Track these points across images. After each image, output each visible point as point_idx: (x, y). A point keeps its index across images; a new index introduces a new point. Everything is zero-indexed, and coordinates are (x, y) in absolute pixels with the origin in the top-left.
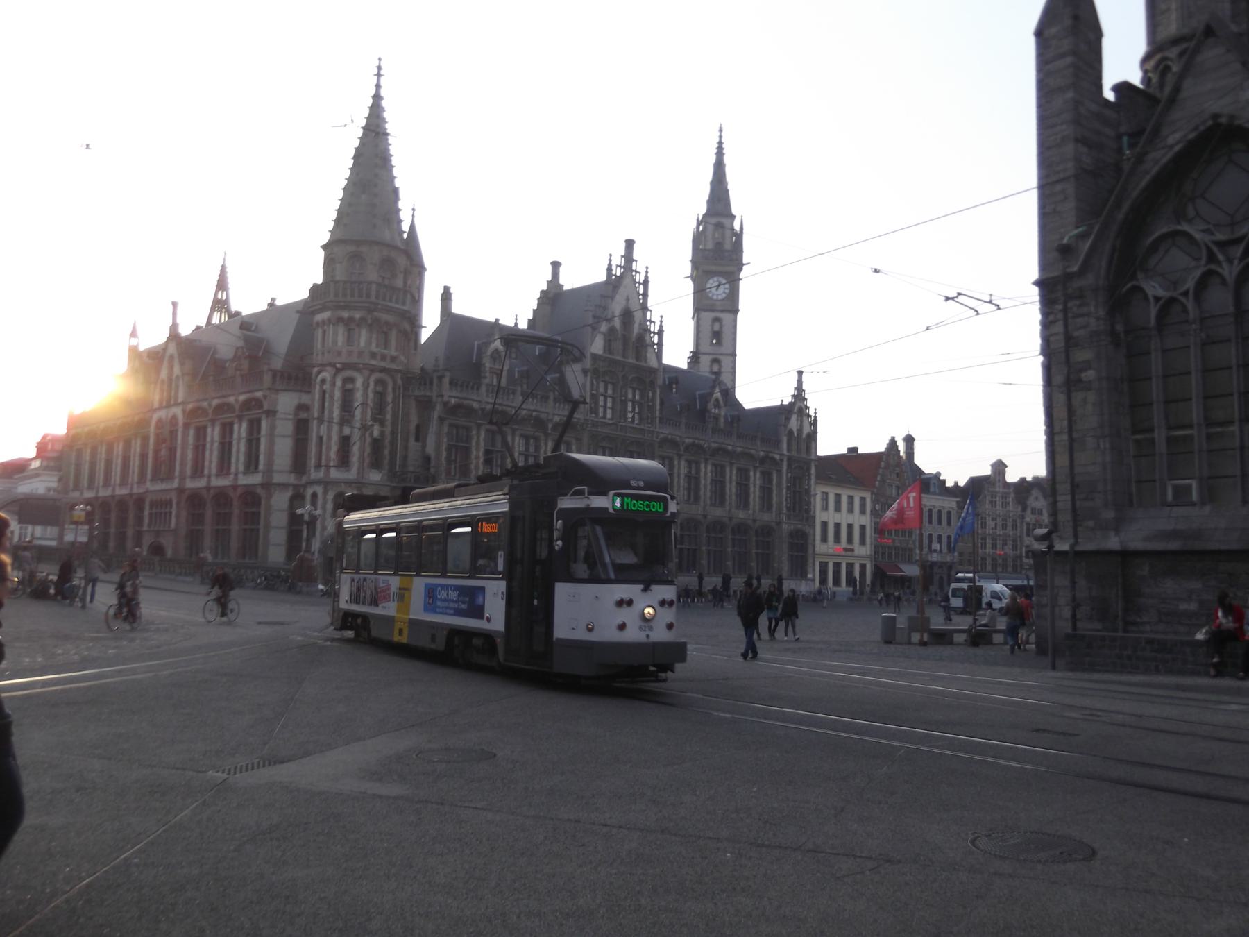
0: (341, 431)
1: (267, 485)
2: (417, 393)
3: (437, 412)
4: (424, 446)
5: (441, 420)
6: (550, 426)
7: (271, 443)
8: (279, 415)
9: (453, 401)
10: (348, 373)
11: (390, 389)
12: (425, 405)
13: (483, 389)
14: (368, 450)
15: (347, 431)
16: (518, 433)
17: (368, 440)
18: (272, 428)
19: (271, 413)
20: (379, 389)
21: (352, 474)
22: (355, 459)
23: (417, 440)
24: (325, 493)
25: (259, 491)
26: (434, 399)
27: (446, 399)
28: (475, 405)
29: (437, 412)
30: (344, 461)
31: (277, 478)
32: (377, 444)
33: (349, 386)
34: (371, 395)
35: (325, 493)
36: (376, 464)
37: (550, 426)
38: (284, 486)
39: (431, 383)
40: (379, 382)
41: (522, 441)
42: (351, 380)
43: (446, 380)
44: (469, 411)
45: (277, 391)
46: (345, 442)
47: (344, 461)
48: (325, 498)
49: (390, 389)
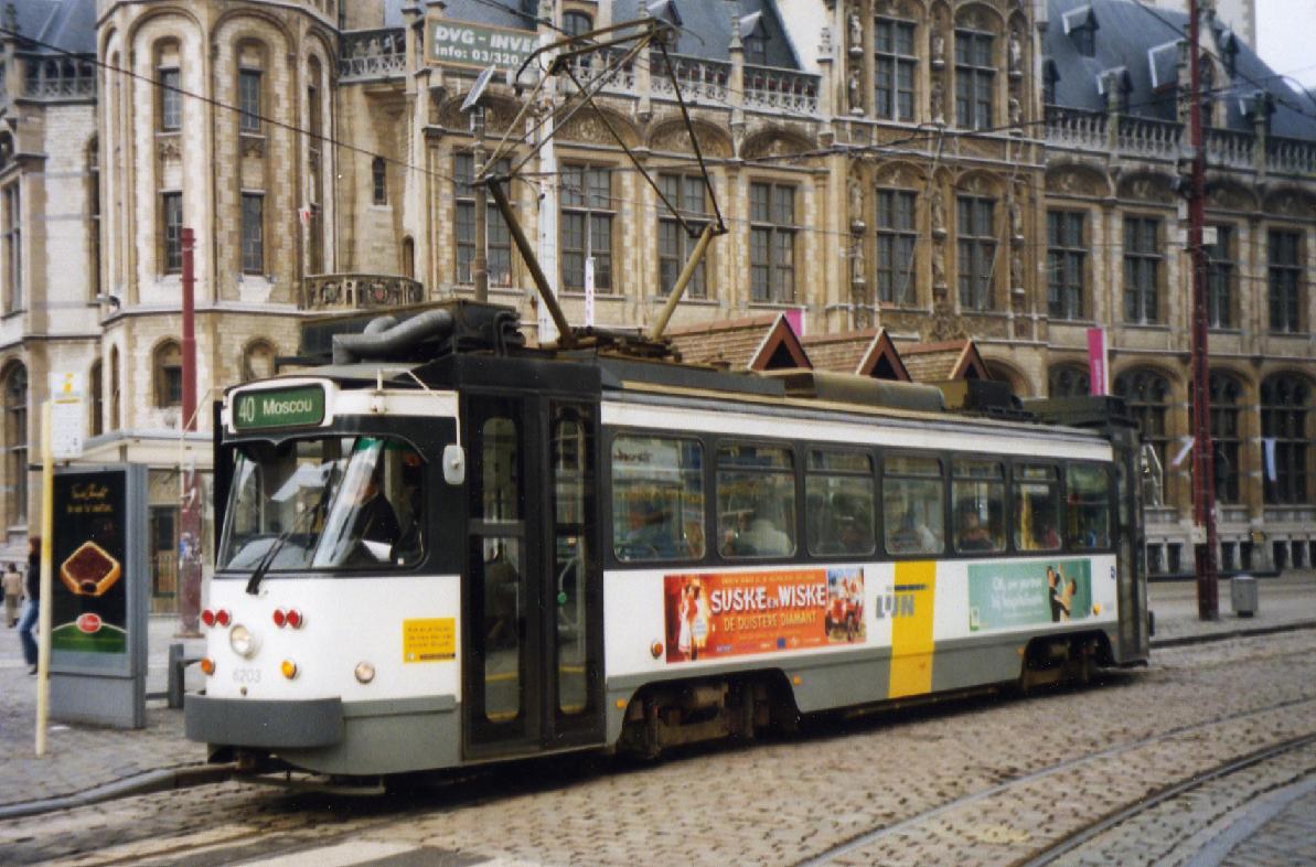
0: (159, 179)
1: (38, 342)
4: (397, 214)
7: (40, 238)
8: (51, 167)
12: (390, 103)
14: (229, 224)
17: (229, 197)
18: (40, 196)
19: (34, 162)
20: (250, 61)
23: (379, 196)
24: (132, 342)
25: (25, 356)
26: (411, 86)
29: (421, 115)
31: (59, 324)
32: (253, 209)
33: (169, 61)
35: (132, 342)
36: (254, 261)
38: (79, 339)
40: (244, 44)
45: (42, 106)
46: (169, 203)
48: (131, 357)
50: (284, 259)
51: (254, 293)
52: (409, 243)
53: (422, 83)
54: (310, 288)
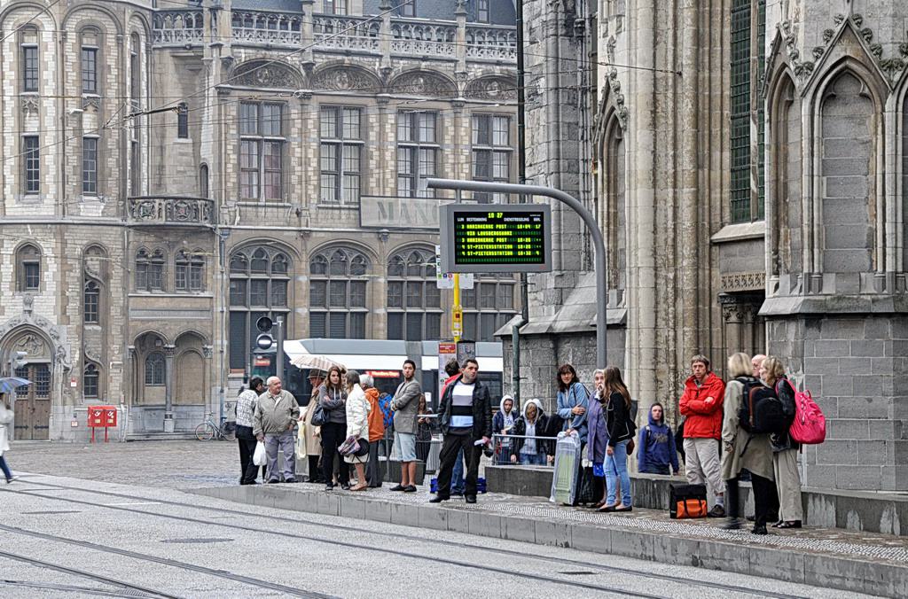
0: (21, 125)
2: (175, 42)
3: (215, 77)
4: (197, 145)
5: (222, 93)
6: (462, 87)
9: (243, 55)
10: (25, 16)
11: (111, 41)
12: (192, 63)
13: (307, 27)
14: (73, 160)
15: (32, 128)
16: (314, 104)
17: (73, 142)
20: (89, 42)
21: (45, 207)
22: (49, 176)
23: (183, 132)
27: (226, 52)
28: (293, 59)
29: (215, 77)
30: (31, 182)
32: (91, 148)
33: (30, 41)
34: (72, 57)
36: (90, 184)
37: (462, 87)
39: (200, 22)
41: (404, 122)
42: (33, 28)
43: (225, 17)
44: (281, 72)
47: (31, 182)
49: (111, 41)
50: (112, 185)
51: (92, 209)
52: (205, 167)
53: (216, 52)
54: (132, 201)
